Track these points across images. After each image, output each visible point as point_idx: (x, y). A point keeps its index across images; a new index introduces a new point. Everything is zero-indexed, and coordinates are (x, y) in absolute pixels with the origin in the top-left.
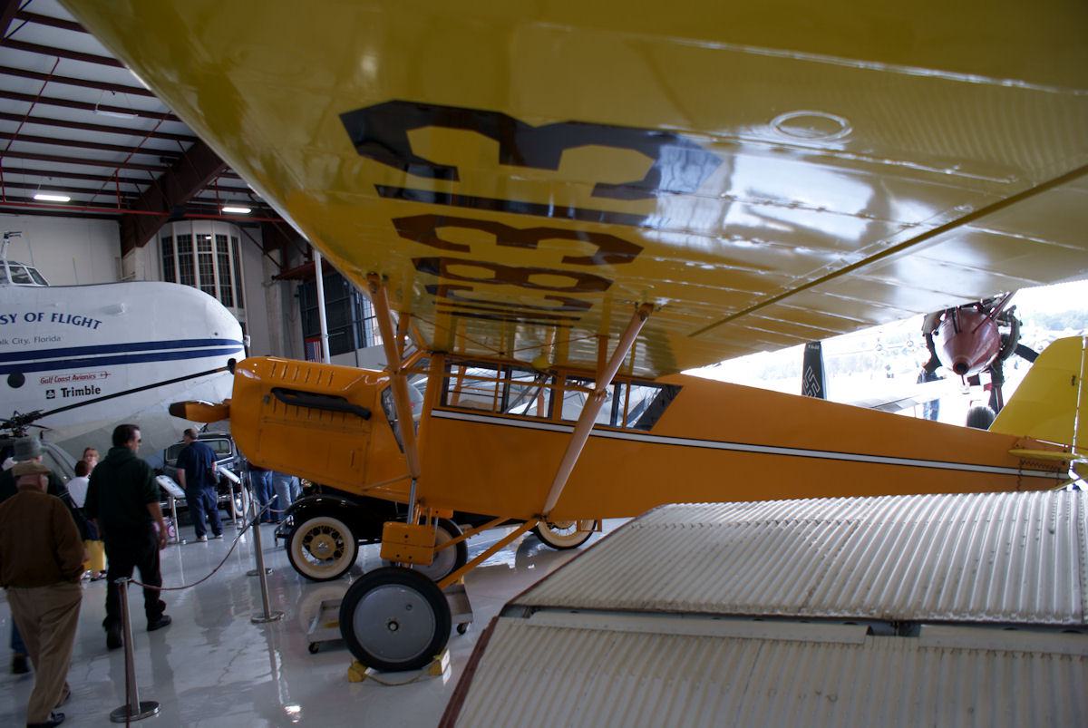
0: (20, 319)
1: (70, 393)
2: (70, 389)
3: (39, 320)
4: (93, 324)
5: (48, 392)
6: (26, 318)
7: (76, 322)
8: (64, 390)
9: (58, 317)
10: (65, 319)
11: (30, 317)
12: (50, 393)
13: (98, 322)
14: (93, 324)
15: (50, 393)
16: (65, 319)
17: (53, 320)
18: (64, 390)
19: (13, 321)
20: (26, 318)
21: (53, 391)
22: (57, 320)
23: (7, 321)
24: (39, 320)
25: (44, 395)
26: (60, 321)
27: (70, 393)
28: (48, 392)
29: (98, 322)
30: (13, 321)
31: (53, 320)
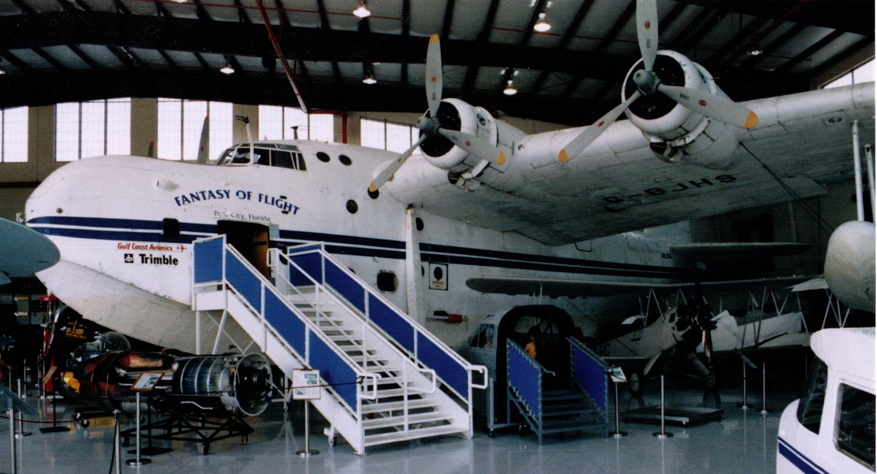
0: (232, 194)
1: (149, 261)
2: (148, 256)
3: (249, 198)
4: (293, 209)
5: (126, 256)
6: (237, 194)
7: (279, 203)
8: (142, 256)
9: (263, 197)
10: (270, 200)
11: (241, 195)
12: (129, 257)
13: (296, 208)
14: (293, 209)
15: (129, 257)
16: (270, 200)
17: (260, 200)
18: (142, 256)
19: (228, 197)
20: (237, 194)
21: (131, 256)
22: (263, 200)
23: (222, 196)
24: (249, 198)
25: (123, 259)
26: (266, 202)
27: (149, 261)
28: (126, 256)
29: (296, 208)
30: (228, 197)
31: (260, 200)
